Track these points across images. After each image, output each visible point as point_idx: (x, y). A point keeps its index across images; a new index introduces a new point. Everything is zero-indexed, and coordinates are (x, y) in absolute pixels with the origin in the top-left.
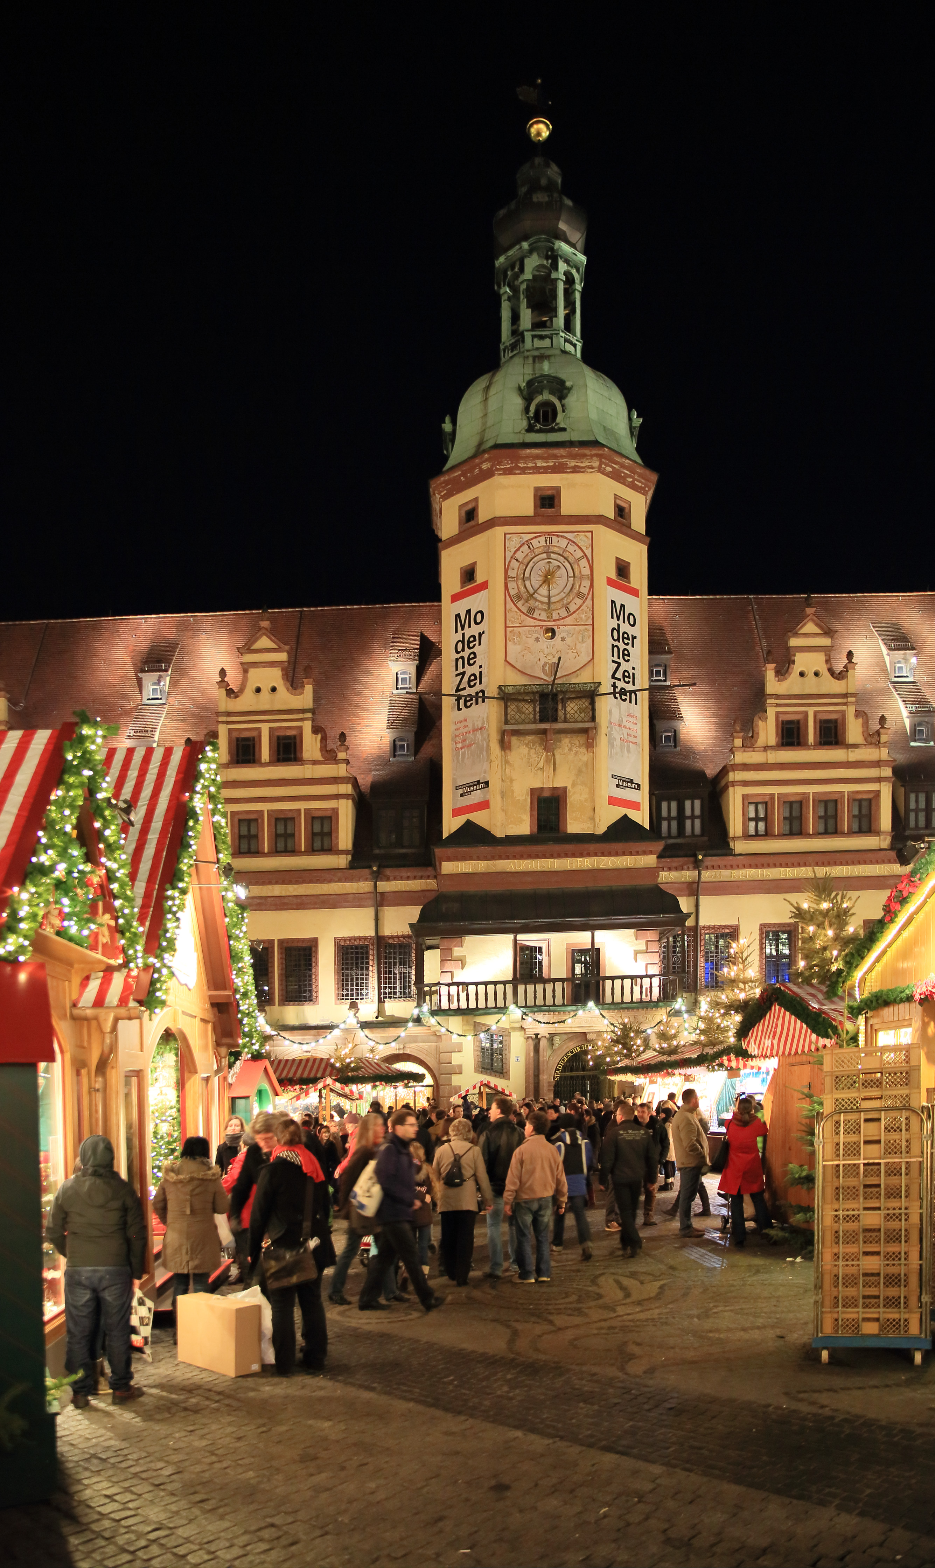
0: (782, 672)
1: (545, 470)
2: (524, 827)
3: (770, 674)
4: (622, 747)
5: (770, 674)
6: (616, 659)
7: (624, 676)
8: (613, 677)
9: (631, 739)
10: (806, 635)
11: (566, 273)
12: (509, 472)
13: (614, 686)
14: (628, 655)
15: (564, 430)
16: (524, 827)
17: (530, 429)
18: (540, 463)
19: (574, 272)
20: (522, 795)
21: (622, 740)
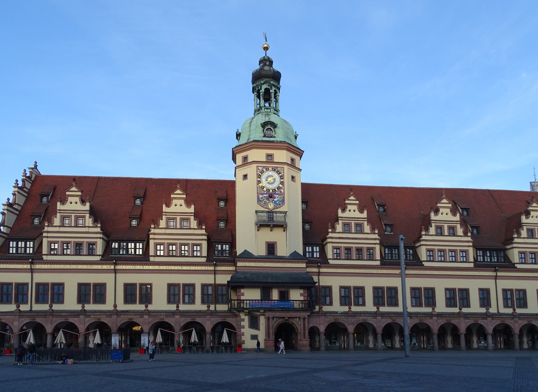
0: (344, 210)
17: (264, 136)
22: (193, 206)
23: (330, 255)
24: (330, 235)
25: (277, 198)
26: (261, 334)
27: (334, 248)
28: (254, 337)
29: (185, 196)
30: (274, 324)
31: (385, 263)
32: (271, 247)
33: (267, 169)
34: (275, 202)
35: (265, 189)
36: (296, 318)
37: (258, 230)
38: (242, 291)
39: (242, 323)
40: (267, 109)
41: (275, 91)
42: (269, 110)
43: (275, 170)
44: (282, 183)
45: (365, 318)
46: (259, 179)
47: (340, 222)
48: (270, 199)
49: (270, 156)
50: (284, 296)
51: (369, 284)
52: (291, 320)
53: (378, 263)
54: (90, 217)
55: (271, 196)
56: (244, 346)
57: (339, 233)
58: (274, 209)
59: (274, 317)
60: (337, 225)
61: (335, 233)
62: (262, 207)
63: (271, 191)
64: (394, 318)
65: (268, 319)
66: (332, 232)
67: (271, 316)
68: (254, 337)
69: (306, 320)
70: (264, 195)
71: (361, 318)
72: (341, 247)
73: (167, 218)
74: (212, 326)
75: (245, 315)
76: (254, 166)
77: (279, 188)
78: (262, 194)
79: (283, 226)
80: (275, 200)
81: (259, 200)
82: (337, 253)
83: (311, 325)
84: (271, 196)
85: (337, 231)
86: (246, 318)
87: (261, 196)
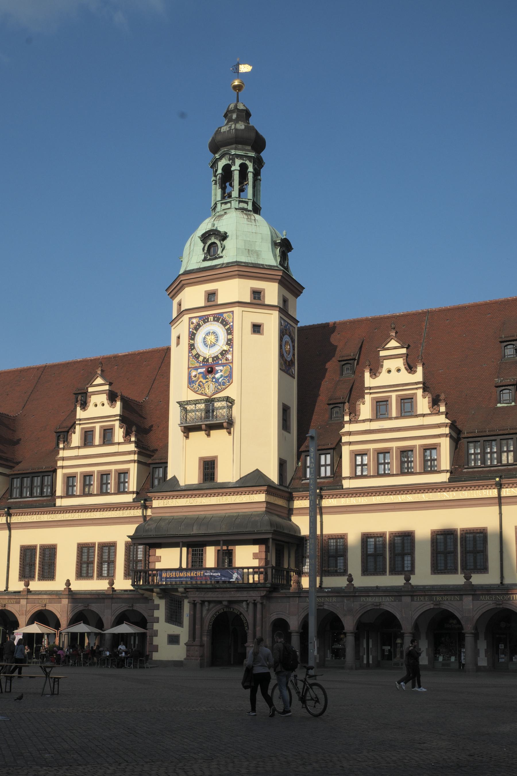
0: (374, 373)
3: (367, 374)
5: (367, 374)
10: (388, 349)
15: (222, 257)
19: (248, 162)
22: (118, 404)
23: (346, 471)
24: (347, 428)
25: (220, 372)
26: (183, 632)
27: (355, 454)
28: (173, 639)
30: (208, 615)
31: (461, 474)
32: (209, 467)
33: (205, 320)
34: (217, 381)
35: (201, 359)
36: (242, 601)
37: (187, 437)
38: (159, 552)
39: (156, 613)
40: (226, 203)
41: (241, 165)
42: (228, 205)
43: (217, 321)
44: (230, 342)
45: (377, 600)
46: (192, 342)
47: (368, 398)
48: (210, 376)
49: (211, 295)
52: (236, 606)
55: (211, 371)
56: (156, 656)
57: (364, 421)
58: (214, 394)
59: (203, 602)
60: (362, 406)
61: (357, 422)
62: (196, 392)
63: (210, 360)
64: (439, 598)
65: (194, 604)
66: (350, 422)
67: (198, 600)
68: (173, 639)
69: (259, 606)
70: (200, 370)
71: (370, 599)
72: (369, 450)
73: (82, 429)
74: (113, 618)
75: (161, 598)
76: (186, 318)
77: (224, 353)
78: (196, 368)
79: (228, 425)
80: (217, 376)
81: (191, 381)
82: (362, 465)
83: (274, 617)
85: (361, 418)
86: (162, 603)
87: (194, 373)
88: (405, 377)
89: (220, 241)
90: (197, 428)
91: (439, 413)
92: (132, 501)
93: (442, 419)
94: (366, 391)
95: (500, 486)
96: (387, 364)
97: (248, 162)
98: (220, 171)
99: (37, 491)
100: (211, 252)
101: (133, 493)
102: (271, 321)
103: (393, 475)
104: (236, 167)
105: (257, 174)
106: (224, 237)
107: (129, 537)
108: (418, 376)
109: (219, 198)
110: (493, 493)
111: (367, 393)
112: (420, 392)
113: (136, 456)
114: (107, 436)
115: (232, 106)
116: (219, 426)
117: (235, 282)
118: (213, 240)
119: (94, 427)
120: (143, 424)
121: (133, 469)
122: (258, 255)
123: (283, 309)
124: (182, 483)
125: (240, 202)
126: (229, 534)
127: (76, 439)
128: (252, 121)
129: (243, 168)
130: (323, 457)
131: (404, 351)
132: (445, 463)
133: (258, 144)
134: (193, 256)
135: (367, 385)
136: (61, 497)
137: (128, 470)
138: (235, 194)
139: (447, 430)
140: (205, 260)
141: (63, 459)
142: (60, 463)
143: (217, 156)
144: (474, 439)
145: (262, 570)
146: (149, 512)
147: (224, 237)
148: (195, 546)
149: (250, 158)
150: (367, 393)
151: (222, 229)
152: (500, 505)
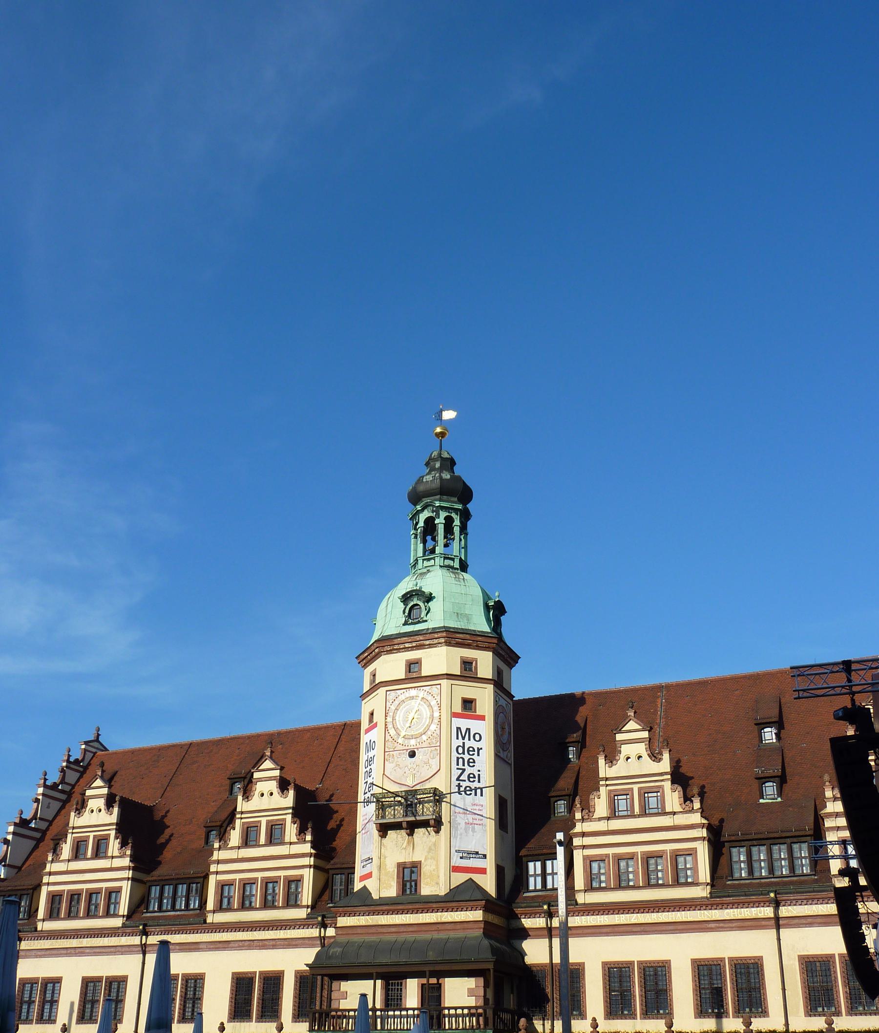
1: (412, 648)
2: (391, 891)
3: (601, 761)
4: (466, 830)
5: (601, 761)
6: (460, 766)
7: (469, 777)
8: (458, 779)
9: (475, 822)
11: (446, 518)
12: (389, 652)
13: (459, 786)
14: (474, 762)
15: (426, 621)
16: (391, 891)
18: (407, 645)
19: (453, 515)
20: (391, 868)
21: (467, 824)
22: (291, 793)
29: (277, 773)
31: (724, 887)
32: (409, 874)
40: (429, 560)
47: (603, 791)
50: (432, 997)
51: (680, 954)
53: (702, 892)
54: (116, 838)
57: (600, 819)
61: (590, 819)
66: (583, 820)
72: (607, 856)
76: (382, 691)
84: (412, 754)
88: (649, 766)
89: (424, 602)
90: (397, 826)
91: (692, 811)
92: (305, 916)
93: (696, 818)
94: (601, 783)
95: (777, 904)
96: (625, 750)
97: (453, 515)
98: (421, 524)
99: (181, 904)
100: (411, 616)
101: (308, 907)
102: (485, 698)
103: (639, 888)
104: (440, 521)
105: (463, 529)
106: (429, 598)
107: (307, 965)
108: (665, 765)
109: (420, 553)
110: (768, 912)
111: (603, 785)
112: (667, 785)
113: (312, 859)
114: (275, 835)
115: (435, 454)
116: (425, 824)
117: (443, 650)
118: (415, 601)
119: (260, 822)
120: (323, 820)
121: (308, 876)
122: (468, 620)
123: (499, 683)
124: (375, 896)
125: (445, 558)
126: (436, 963)
127: (235, 836)
128: (458, 471)
129: (449, 521)
130: (531, 865)
131: (645, 734)
132: (704, 873)
133: (465, 494)
134: (390, 618)
135: (602, 774)
136: (214, 912)
137: (302, 876)
138: (439, 549)
139: (704, 833)
140: (405, 624)
141: (218, 862)
142: (213, 868)
143: (419, 508)
144: (738, 843)
145: (480, 1011)
146: (331, 932)
147: (429, 598)
148: (393, 980)
149: (456, 511)
150: (603, 785)
151: (426, 590)
152: (778, 927)
